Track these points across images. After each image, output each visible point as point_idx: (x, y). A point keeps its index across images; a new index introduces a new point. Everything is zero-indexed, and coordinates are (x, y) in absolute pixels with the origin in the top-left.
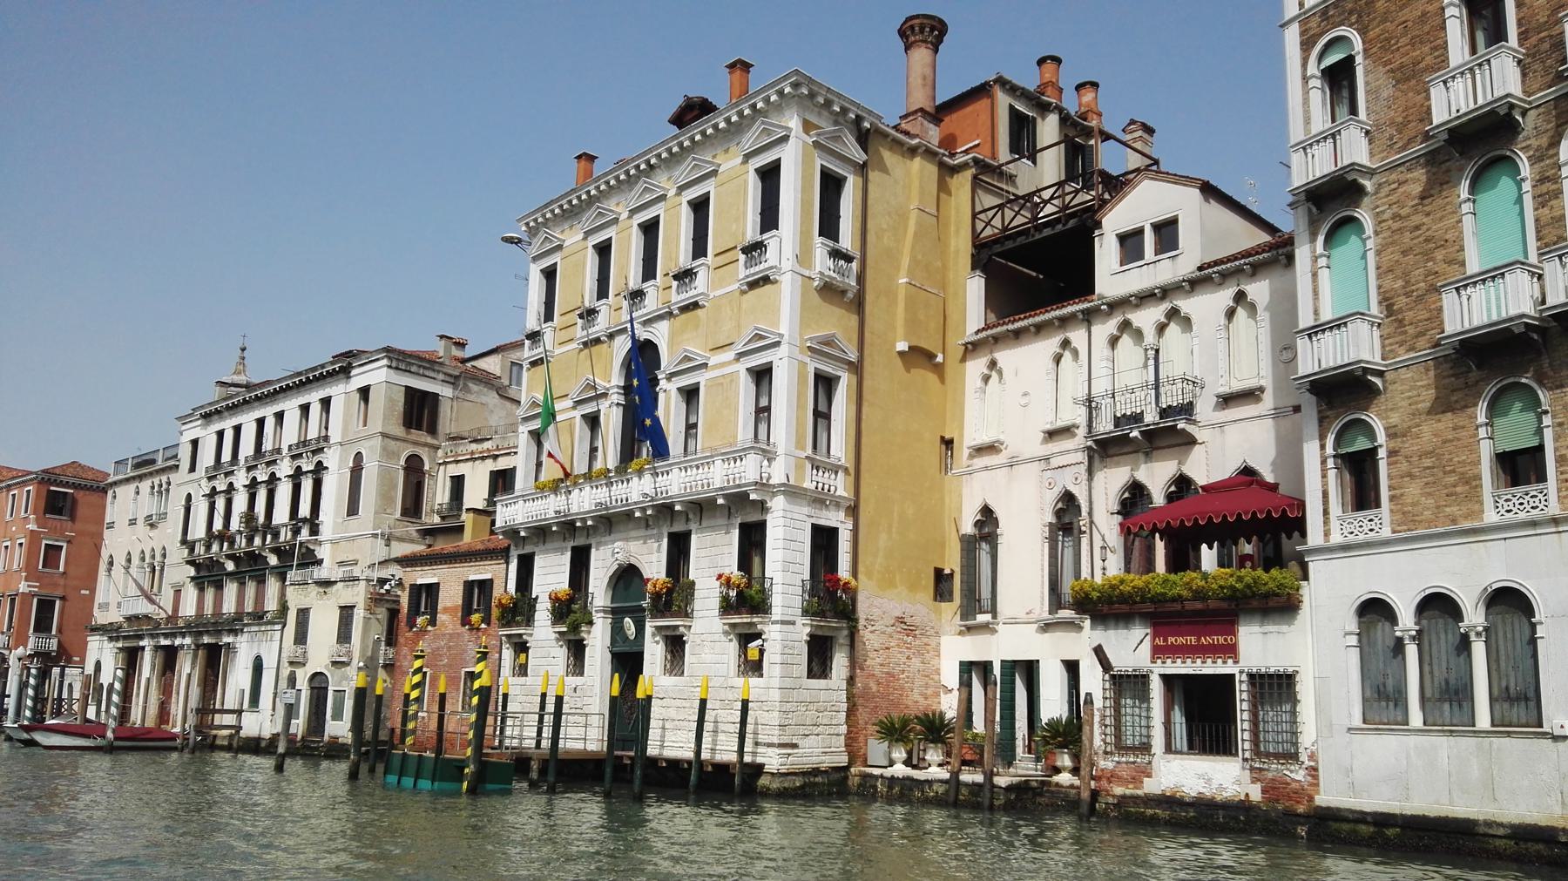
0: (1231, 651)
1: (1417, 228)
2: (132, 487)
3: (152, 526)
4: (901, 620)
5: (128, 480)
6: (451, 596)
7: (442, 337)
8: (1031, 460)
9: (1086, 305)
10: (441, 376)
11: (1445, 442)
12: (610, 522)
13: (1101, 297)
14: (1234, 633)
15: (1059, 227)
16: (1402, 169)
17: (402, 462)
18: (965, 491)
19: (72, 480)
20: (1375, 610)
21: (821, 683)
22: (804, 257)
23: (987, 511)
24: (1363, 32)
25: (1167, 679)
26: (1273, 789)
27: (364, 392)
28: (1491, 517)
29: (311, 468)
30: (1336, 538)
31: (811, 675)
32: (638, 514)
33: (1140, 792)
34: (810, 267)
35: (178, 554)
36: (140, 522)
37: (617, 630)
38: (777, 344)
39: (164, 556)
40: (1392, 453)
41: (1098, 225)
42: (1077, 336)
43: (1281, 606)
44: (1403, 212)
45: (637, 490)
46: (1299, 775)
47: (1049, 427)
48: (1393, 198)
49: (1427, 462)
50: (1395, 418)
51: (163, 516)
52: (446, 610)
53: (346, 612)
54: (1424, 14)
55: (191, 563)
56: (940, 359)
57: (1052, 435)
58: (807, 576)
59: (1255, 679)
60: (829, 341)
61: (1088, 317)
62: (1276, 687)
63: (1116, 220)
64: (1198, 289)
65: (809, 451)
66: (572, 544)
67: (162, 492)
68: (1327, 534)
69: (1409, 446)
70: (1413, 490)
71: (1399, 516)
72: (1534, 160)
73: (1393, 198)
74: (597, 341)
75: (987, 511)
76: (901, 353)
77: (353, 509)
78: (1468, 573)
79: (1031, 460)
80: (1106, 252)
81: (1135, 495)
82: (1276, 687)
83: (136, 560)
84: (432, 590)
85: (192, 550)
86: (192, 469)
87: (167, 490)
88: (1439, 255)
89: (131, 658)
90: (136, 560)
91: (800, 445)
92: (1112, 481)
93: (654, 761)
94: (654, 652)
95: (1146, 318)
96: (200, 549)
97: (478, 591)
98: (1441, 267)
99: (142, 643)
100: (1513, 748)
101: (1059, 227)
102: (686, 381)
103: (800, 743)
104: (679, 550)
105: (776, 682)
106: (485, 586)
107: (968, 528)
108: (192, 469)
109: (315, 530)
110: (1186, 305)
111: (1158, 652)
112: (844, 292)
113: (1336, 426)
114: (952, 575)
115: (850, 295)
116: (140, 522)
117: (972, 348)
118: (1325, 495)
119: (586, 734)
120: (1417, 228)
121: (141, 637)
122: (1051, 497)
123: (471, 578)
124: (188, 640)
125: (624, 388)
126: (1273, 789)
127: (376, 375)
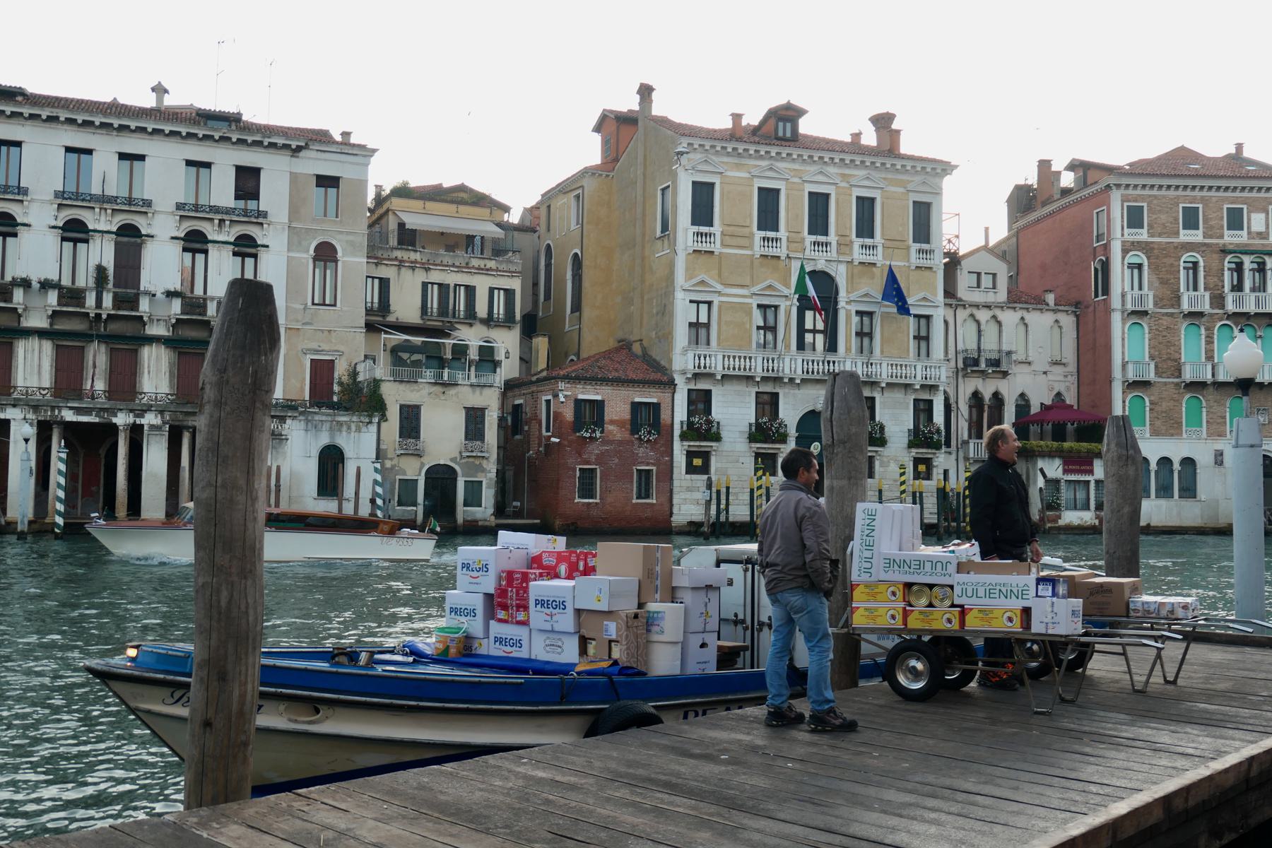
0: (1091, 472)
13: (961, 300)
14: (1091, 464)
24: (1148, 258)
52: (612, 422)
69: (1158, 408)
70: (1158, 423)
72: (1207, 329)
74: (778, 257)
81: (976, 396)
92: (968, 387)
95: (983, 315)
100: (1188, 504)
111: (1065, 471)
113: (1130, 396)
123: (637, 400)
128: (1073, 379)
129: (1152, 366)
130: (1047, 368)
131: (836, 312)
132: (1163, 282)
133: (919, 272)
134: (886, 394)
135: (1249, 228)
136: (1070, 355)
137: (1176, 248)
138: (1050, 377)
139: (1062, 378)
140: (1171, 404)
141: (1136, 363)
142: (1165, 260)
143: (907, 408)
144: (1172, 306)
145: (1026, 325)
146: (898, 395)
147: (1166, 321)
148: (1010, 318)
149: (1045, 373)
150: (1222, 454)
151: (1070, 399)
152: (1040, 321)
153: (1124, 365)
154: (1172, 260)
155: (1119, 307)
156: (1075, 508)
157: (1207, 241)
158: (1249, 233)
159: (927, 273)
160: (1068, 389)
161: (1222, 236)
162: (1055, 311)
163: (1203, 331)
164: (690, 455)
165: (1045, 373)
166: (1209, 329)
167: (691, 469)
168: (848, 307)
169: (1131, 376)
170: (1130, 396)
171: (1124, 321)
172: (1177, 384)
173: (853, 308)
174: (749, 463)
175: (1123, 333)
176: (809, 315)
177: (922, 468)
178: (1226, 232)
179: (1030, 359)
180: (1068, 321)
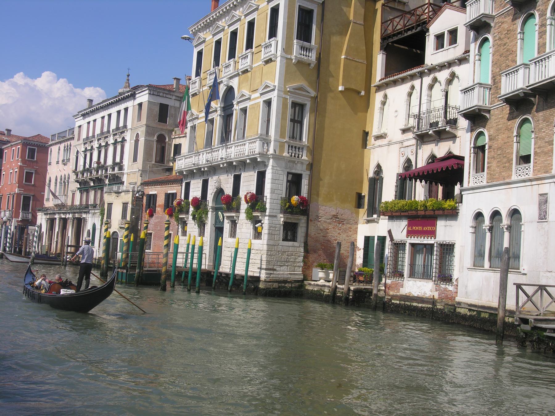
0: (433, 234)
2: (57, 146)
3: (65, 164)
4: (335, 216)
5: (56, 144)
6: (161, 200)
7: (175, 79)
8: (396, 143)
9: (419, 69)
10: (174, 97)
11: (505, 143)
12: (214, 169)
14: (435, 225)
15: (414, 31)
16: (503, 16)
17: (155, 138)
18: (372, 157)
19: (36, 143)
21: (291, 243)
22: (287, 49)
23: (379, 167)
25: (413, 245)
27: (140, 105)
28: (514, 178)
29: (120, 140)
30: (472, 185)
31: (285, 239)
33: (398, 294)
34: (291, 53)
35: (73, 177)
36: (60, 162)
37: (217, 217)
38: (273, 90)
39: (69, 178)
40: (490, 147)
41: (428, 30)
42: (417, 83)
43: (453, 214)
45: (221, 154)
46: (450, 288)
47: (403, 127)
49: (499, 152)
51: (69, 160)
52: (159, 206)
53: (125, 205)
55: (77, 181)
56: (363, 93)
57: (404, 131)
58: (284, 196)
60: (301, 89)
61: (421, 75)
62: (447, 249)
63: (435, 29)
64: (443, 68)
65: (287, 139)
67: (68, 149)
75: (379, 167)
76: (341, 91)
77: (135, 160)
79: (396, 143)
80: (430, 43)
82: (447, 249)
83: (59, 180)
84: (155, 196)
85: (77, 175)
86: (79, 140)
87: (70, 149)
89: (51, 222)
90: (59, 180)
91: (282, 135)
93: (221, 273)
94: (227, 226)
95: (443, 75)
96: (80, 176)
97: (170, 197)
99: (55, 217)
101: (414, 31)
102: (242, 106)
103: (278, 269)
105: (265, 242)
106: (174, 195)
107: (371, 175)
108: (79, 140)
109: (121, 168)
110: (457, 69)
111: (410, 233)
112: (309, 64)
114: (364, 196)
115: (312, 65)
116: (60, 162)
117: (379, 88)
121: (55, 214)
122: (403, 160)
123: (169, 192)
124: (71, 216)
125: (223, 107)
127: (143, 97)
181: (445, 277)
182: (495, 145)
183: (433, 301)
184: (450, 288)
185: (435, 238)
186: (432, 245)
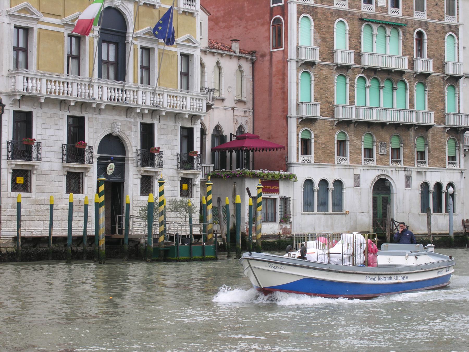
0: (277, 191)
1: (324, 83)
11: (327, 142)
14: (278, 185)
20: (309, 182)
24: (314, 20)
26: (284, 230)
32: (139, 111)
40: (315, 141)
44: (321, 78)
46: (288, 226)
48: (319, 72)
49: (323, 146)
50: (316, 132)
54: (329, 26)
59: (281, 199)
66: (68, 113)
68: (298, 160)
69: (319, 141)
70: (320, 152)
71: (316, 158)
72: (350, 80)
73: (319, 72)
78: (331, 175)
82: (285, 201)
88: (329, 93)
98: (329, 97)
100: (338, 217)
104: (147, 132)
118: (298, 149)
119: (86, 224)
120: (324, 83)
126: (284, 230)
128: (250, 115)
129: (318, 107)
130: (233, 105)
131: (125, 45)
132: (324, 40)
133: (184, 16)
134: (162, 122)
135: (376, 3)
136: (247, 96)
137: (331, 14)
138: (236, 113)
139: (242, 114)
140: (328, 137)
141: (309, 104)
142: (325, 23)
143: (176, 135)
144: (329, 60)
145: (220, 68)
146: (170, 123)
147: (325, 71)
148: (210, 62)
149: (233, 109)
150: (359, 178)
151: (248, 129)
152: (230, 66)
153: (299, 105)
154: (328, 23)
155: (295, 58)
156: (267, 221)
157: (351, 10)
158: (376, 7)
159: (189, 17)
160: (247, 122)
161: (360, 8)
162: (239, 58)
163: (348, 81)
164: (16, 173)
165: (233, 109)
166: (352, 80)
167: (16, 187)
168: (135, 42)
169: (305, 114)
170: (302, 130)
171: (298, 69)
172: (332, 122)
173: (139, 44)
174: (63, 182)
175: (298, 79)
176: (104, 46)
177: (185, 187)
178: (363, 5)
179: (223, 97)
180: (247, 67)
181: (285, 219)
182: (319, 141)
183: (278, 236)
184: (288, 226)
185: (279, 194)
186: (275, 199)
